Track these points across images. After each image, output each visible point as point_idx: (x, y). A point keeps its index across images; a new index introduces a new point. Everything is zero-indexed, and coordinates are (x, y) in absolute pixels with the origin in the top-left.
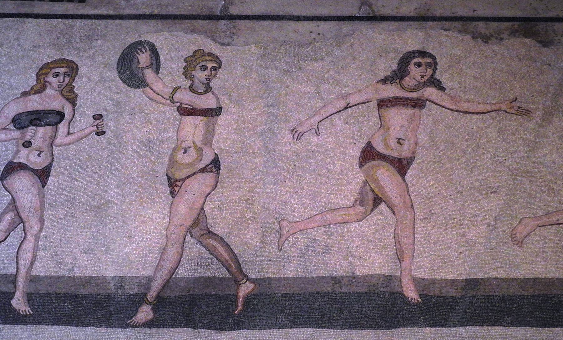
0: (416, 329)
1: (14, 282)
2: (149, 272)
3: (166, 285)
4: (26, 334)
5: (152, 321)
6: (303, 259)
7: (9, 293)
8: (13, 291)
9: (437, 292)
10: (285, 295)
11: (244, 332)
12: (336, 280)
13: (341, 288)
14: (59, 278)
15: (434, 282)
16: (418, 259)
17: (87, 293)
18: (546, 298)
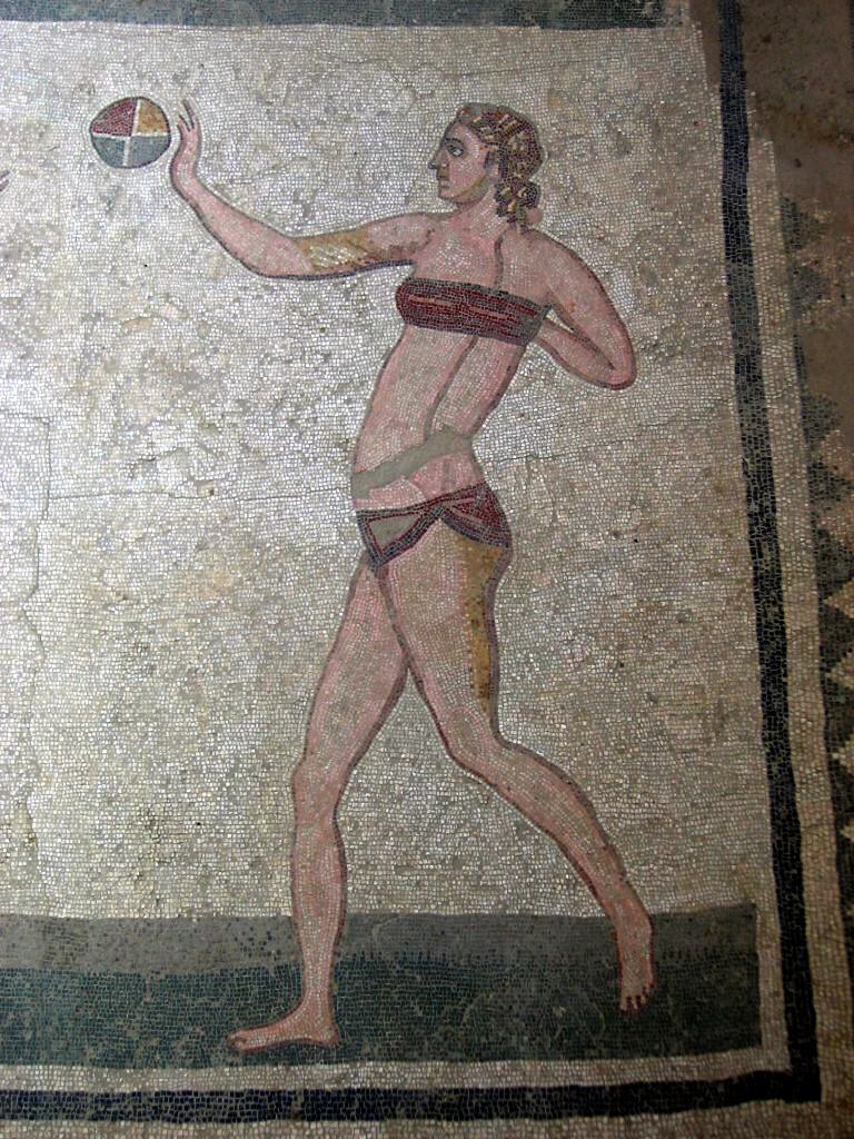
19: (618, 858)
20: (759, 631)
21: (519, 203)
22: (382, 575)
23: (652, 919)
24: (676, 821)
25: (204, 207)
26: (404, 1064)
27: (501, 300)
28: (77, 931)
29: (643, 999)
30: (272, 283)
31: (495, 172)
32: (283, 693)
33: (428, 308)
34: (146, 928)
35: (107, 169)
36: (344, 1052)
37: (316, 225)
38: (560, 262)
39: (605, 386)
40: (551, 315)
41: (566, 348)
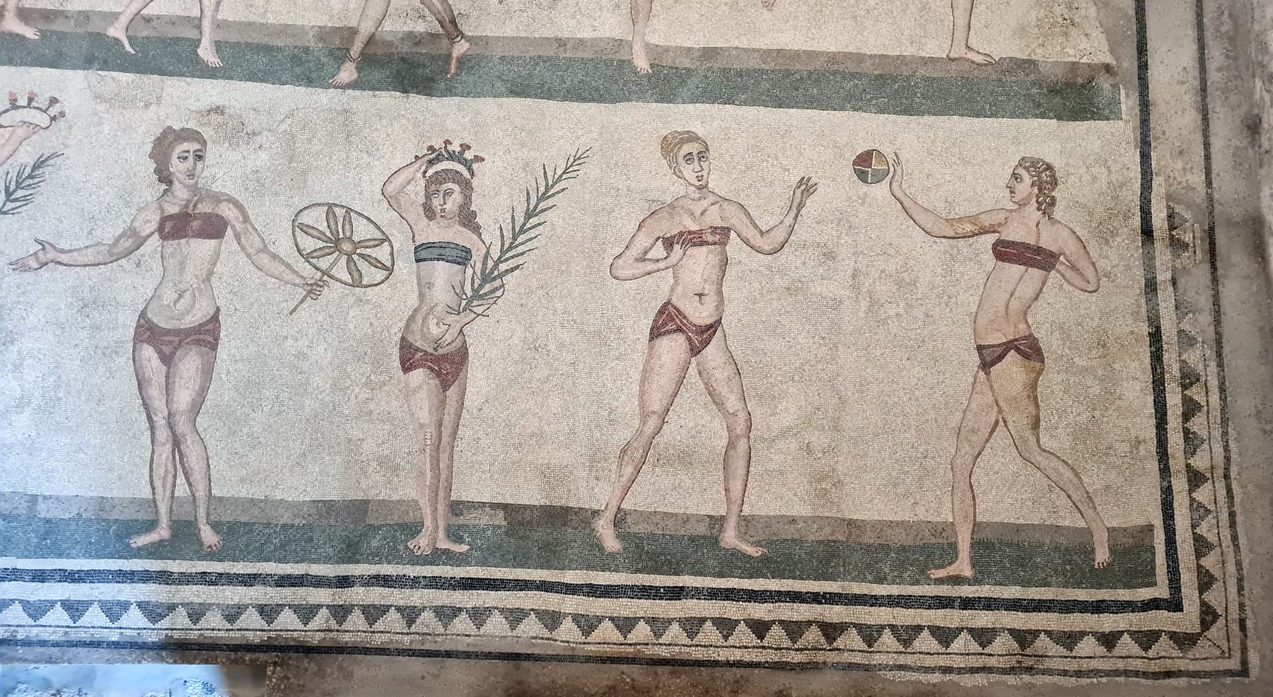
0: (642, 104)
1: (199, 27)
2: (353, 23)
3: (371, 40)
4: (218, 90)
5: (356, 81)
6: (525, 14)
7: (194, 41)
8: (199, 37)
9: (670, 62)
10: (502, 58)
11: (456, 99)
12: (561, 43)
13: (565, 52)
14: (250, 24)
15: (667, 50)
16: (654, 21)
17: (282, 45)
18: (787, 74)
19: (1093, 502)
20: (1155, 405)
21: (1047, 206)
22: (988, 374)
23: (1108, 529)
24: (1118, 487)
25: (906, 204)
26: (1002, 587)
27: (1038, 250)
28: (861, 525)
29: (1105, 564)
30: (937, 239)
31: (1036, 190)
32: (946, 424)
33: (1006, 253)
34: (891, 524)
35: (860, 183)
36: (976, 581)
37: (956, 214)
38: (1065, 233)
39: (1086, 291)
40: (1062, 258)
41: (1070, 274)
